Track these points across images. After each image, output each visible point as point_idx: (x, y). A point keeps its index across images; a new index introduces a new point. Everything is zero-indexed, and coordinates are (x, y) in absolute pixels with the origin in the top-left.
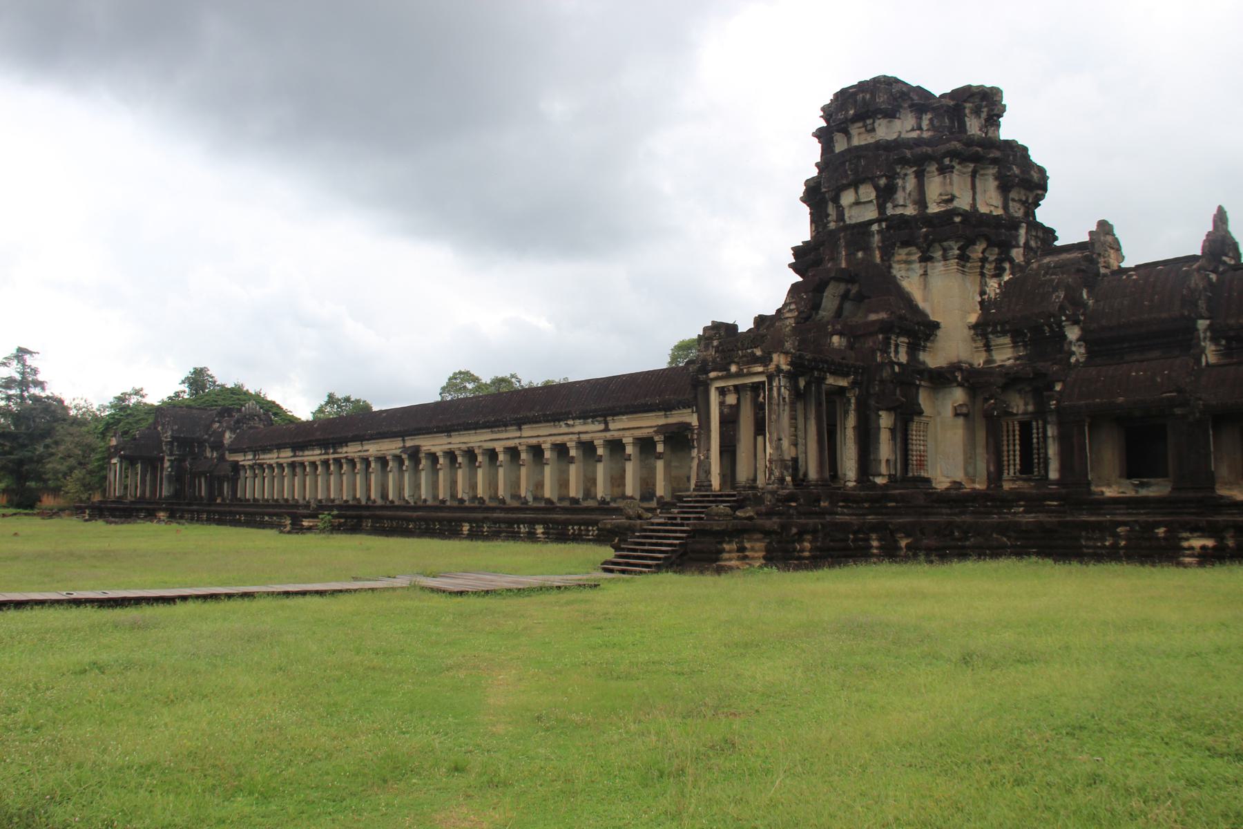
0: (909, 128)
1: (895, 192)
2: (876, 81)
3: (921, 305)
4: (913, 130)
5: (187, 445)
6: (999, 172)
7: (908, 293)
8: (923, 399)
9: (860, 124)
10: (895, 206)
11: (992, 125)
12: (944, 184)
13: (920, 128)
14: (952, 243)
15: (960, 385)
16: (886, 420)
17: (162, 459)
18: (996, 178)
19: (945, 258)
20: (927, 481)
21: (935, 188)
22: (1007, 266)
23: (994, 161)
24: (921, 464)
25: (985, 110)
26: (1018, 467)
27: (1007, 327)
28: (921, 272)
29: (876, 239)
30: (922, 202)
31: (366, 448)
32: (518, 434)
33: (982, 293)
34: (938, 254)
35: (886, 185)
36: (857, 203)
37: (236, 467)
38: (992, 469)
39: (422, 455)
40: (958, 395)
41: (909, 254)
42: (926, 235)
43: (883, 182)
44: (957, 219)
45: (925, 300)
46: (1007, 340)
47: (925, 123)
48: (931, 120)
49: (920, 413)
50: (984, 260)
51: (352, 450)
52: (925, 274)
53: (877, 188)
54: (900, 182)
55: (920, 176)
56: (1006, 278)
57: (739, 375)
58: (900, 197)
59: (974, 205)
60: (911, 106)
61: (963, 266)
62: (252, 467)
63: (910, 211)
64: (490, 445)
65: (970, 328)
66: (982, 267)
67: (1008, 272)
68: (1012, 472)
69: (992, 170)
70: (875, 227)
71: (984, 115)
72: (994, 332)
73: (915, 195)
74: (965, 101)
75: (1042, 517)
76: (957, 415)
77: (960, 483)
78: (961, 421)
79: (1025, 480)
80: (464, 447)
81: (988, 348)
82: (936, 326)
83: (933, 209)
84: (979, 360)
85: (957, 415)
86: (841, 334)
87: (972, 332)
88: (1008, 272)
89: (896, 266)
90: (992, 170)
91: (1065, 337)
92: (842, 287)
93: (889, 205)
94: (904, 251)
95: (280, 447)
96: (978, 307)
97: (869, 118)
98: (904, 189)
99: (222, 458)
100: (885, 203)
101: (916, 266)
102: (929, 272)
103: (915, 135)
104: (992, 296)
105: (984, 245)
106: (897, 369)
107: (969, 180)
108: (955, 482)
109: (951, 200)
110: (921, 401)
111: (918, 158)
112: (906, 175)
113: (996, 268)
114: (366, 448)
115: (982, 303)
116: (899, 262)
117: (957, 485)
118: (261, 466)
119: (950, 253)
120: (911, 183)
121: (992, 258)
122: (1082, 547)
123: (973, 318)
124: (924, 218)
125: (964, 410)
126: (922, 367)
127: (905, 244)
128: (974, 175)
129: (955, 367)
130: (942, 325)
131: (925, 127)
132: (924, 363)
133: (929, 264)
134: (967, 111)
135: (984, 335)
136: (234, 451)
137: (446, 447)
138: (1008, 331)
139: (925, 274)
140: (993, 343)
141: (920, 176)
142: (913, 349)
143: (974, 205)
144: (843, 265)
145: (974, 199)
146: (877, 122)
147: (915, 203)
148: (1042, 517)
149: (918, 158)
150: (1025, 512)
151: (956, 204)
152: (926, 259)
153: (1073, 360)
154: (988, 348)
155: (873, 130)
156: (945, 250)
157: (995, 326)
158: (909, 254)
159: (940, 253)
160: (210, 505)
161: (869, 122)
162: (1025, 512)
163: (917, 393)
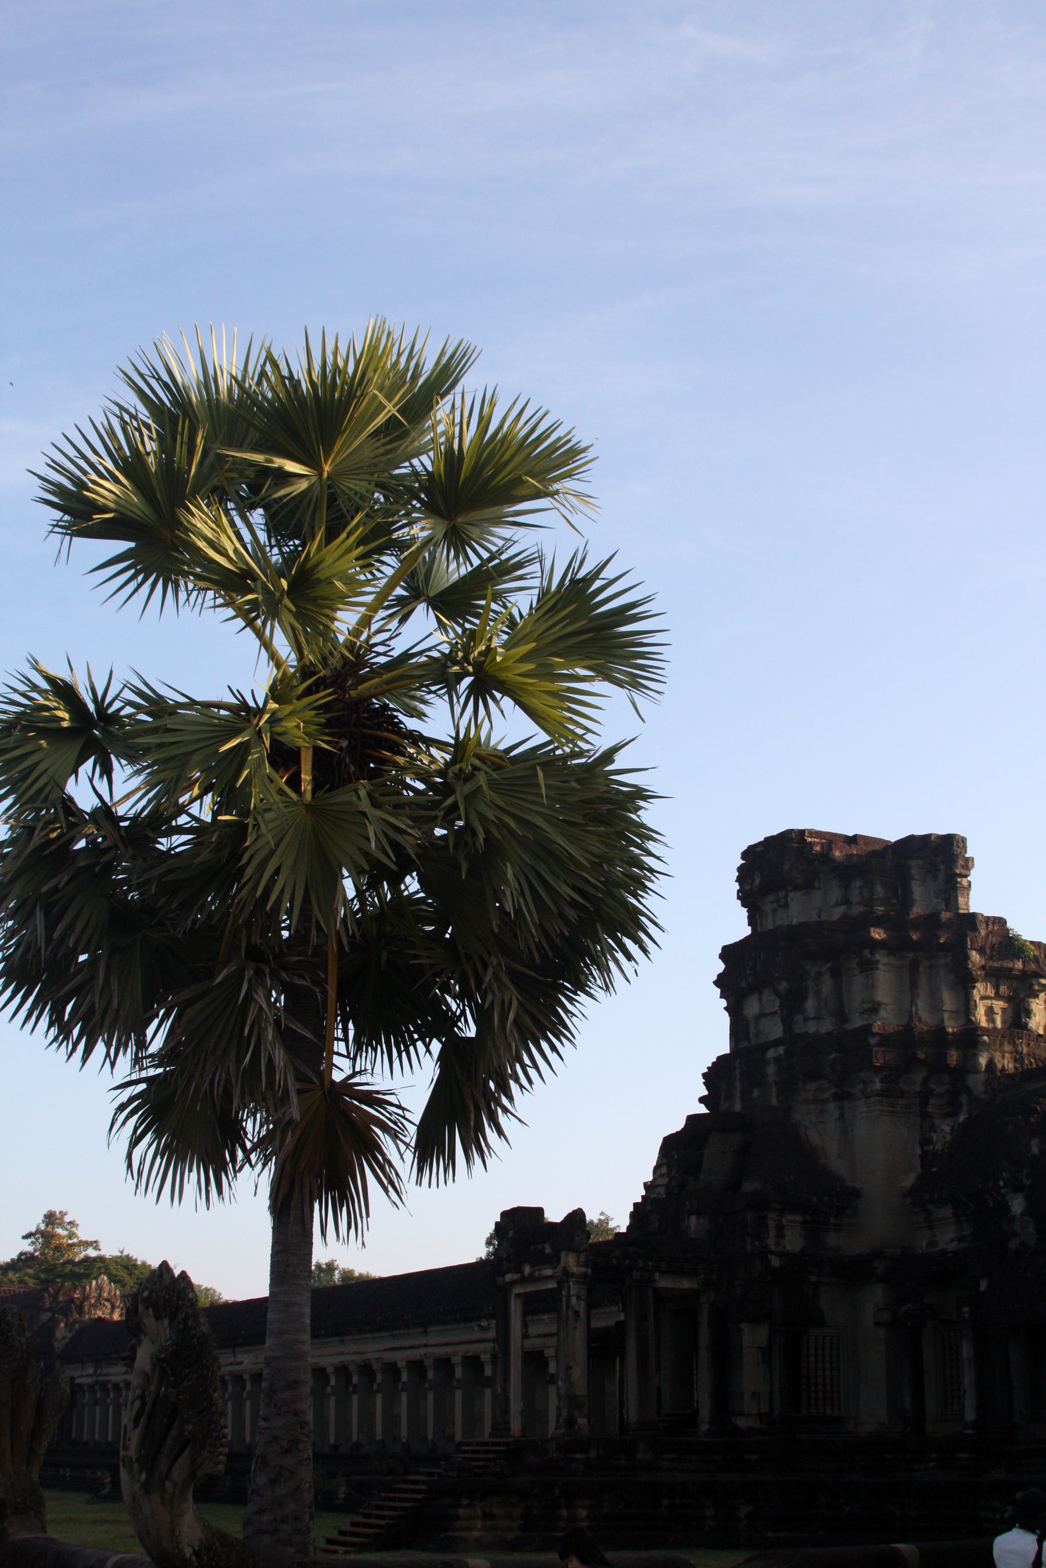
9: (772, 898)
22: (964, 1099)
28: (836, 1115)
29: (771, 1070)
31: (239, 1358)
32: (422, 1341)
33: (925, 1142)
36: (763, 1015)
43: (783, 986)
46: (947, 1212)
52: (841, 1117)
53: (778, 994)
55: (836, 974)
56: (962, 1118)
57: (532, 1279)
58: (810, 1005)
62: (91, 1387)
64: (389, 1356)
67: (965, 1108)
70: (771, 1054)
71: (941, 875)
76: (877, 1324)
80: (358, 1358)
85: (877, 1324)
86: (699, 1213)
88: (965, 1108)
91: (1007, 1208)
94: (812, 1086)
96: (918, 1164)
98: (818, 994)
101: (832, 1106)
104: (939, 1147)
105: (923, 1073)
114: (239, 1358)
115: (923, 1156)
118: (103, 1385)
120: (827, 985)
123: (909, 1181)
128: (914, 967)
134: (915, 872)
137: (337, 1359)
144: (738, 1108)
146: (791, 895)
152: (842, 1097)
153: (1013, 1244)
155: (786, 906)
161: (782, 894)
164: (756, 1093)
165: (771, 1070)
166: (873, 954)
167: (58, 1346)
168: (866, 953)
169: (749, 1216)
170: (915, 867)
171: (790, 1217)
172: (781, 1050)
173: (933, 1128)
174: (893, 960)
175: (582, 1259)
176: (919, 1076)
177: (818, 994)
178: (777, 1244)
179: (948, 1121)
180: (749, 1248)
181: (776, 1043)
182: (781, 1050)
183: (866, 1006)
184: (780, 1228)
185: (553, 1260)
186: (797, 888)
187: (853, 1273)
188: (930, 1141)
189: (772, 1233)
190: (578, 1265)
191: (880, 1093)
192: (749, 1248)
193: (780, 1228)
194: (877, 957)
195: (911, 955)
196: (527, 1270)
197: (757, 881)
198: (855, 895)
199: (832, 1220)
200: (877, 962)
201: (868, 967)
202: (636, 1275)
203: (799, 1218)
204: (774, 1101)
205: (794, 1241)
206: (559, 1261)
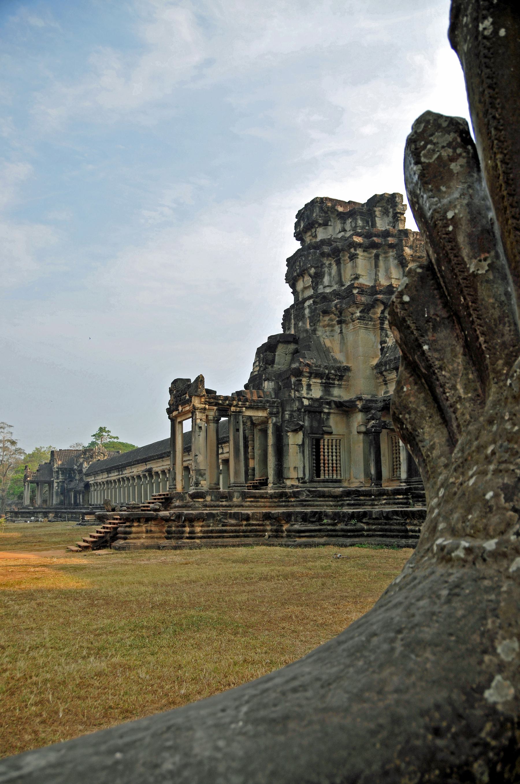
2: (313, 202)
4: (340, 232)
5: (68, 472)
8: (335, 423)
9: (309, 234)
10: (324, 287)
13: (344, 230)
15: (361, 411)
16: (294, 440)
17: (53, 481)
18: (395, 258)
24: (335, 470)
25: (391, 210)
27: (392, 366)
28: (339, 331)
29: (307, 311)
33: (383, 342)
35: (316, 273)
37: (87, 486)
39: (153, 473)
44: (355, 291)
47: (348, 227)
50: (382, 320)
51: (127, 473)
52: (341, 332)
53: (310, 275)
54: (326, 269)
55: (338, 263)
58: (326, 280)
61: (367, 324)
66: (382, 323)
69: (392, 253)
71: (391, 214)
72: (386, 370)
73: (337, 279)
82: (348, 369)
87: (375, 371)
89: (320, 329)
90: (392, 253)
92: (292, 347)
93: (321, 287)
94: (327, 318)
95: (102, 471)
97: (312, 228)
98: (330, 274)
99: (81, 480)
100: (317, 284)
102: (344, 331)
105: (382, 308)
106: (306, 402)
109: (357, 278)
111: (339, 251)
115: (382, 349)
116: (324, 326)
122: (407, 531)
123: (375, 362)
125: (363, 429)
127: (326, 312)
128: (377, 257)
131: (348, 230)
133: (344, 326)
134: (377, 213)
135: (381, 373)
136: (88, 475)
137: (161, 468)
139: (341, 332)
142: (327, 387)
144: (293, 332)
145: (376, 275)
146: (318, 230)
149: (339, 251)
151: (361, 281)
155: (316, 236)
160: (74, 509)
161: (313, 230)
163: (328, 419)
164: (300, 324)
165: (307, 311)
166: (355, 250)
167: (84, 470)
168: (352, 250)
169: (293, 380)
170: (378, 211)
171: (314, 380)
172: (311, 301)
173: (387, 336)
174: (365, 254)
175: (203, 400)
176: (379, 309)
177: (330, 274)
178: (308, 394)
180: (293, 396)
181: (309, 298)
182: (311, 301)
183: (353, 277)
184: (309, 386)
185: (189, 401)
186: (320, 225)
187: (346, 409)
188: (385, 342)
189: (305, 388)
190: (201, 403)
191: (360, 318)
192: (293, 396)
193: (309, 386)
194: (358, 252)
195: (375, 251)
196: (180, 408)
197: (302, 226)
198: (348, 227)
199: (336, 382)
201: (353, 257)
202: (233, 409)
203: (319, 381)
204: (308, 327)
205: (317, 393)
206: (191, 402)
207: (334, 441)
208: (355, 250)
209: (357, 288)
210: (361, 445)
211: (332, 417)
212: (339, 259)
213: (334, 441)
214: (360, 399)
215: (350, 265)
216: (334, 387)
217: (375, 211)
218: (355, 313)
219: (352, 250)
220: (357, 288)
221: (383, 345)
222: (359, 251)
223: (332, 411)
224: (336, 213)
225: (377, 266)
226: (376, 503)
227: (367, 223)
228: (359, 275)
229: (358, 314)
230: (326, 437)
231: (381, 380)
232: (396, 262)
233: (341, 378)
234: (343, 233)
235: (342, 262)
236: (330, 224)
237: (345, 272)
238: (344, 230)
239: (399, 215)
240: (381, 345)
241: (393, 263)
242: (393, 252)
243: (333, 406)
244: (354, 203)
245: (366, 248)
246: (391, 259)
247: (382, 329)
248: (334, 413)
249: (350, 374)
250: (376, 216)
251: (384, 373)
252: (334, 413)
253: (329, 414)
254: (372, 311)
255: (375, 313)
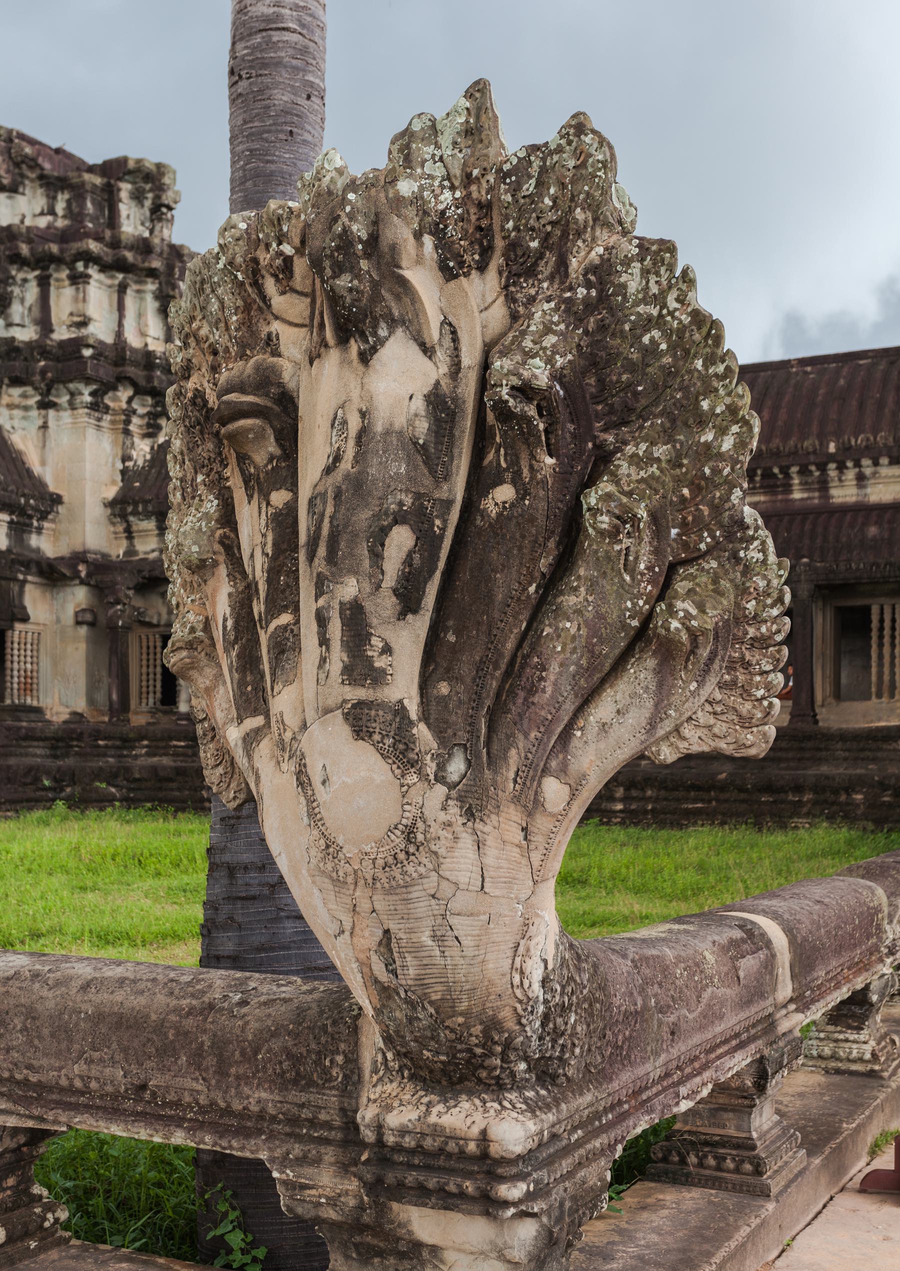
0: (38, 211)
1: (9, 304)
3: (37, 469)
4: (42, 214)
6: (160, 289)
7: (19, 453)
11: (160, 220)
12: (76, 300)
14: (81, 386)
15: (82, 582)
19: (72, 406)
20: (38, 711)
21: (63, 302)
23: (152, 273)
25: (150, 195)
26: (159, 695)
28: (40, 422)
30: (45, 323)
33: (125, 458)
34: (64, 399)
38: (115, 697)
40: (78, 596)
41: (24, 396)
42: (43, 372)
44: (87, 353)
45: (43, 463)
47: (60, 207)
48: (69, 202)
49: (25, 619)
54: (16, 291)
55: (44, 283)
59: (119, 333)
60: (41, 177)
63: (26, 334)
65: (105, 505)
66: (128, 422)
68: (151, 701)
69: (151, 286)
71: (148, 203)
72: (135, 513)
73: (36, 312)
74: (120, 179)
75: (166, 761)
77: (81, 715)
78: (83, 630)
79: (165, 713)
81: (129, 534)
82: (57, 500)
83: (62, 334)
84: (118, 550)
85: (78, 623)
94: (16, 392)
98: (22, 301)
101: (34, 413)
102: (51, 423)
103: (43, 222)
104: (140, 463)
105: (130, 392)
107: (115, 296)
108: (74, 714)
109: (84, 323)
110: (28, 602)
112: (25, 280)
113: (149, 425)
115: (124, 472)
117: (77, 716)
119: (78, 399)
120: (32, 293)
121: (141, 411)
123: (111, 493)
124: (39, 348)
126: (33, 556)
127: (16, 382)
128: (122, 289)
129: (79, 557)
130: (65, 499)
132: (38, 550)
133: (51, 413)
135: (124, 516)
138: (153, 513)
139: (45, 427)
140: (134, 528)
141: (44, 283)
143: (119, 333)
145: (120, 324)
147: (36, 322)
148: (166, 761)
150: (148, 754)
152: (45, 405)
154: (129, 534)
156: (72, 394)
157: (136, 504)
158: (24, 396)
159: (67, 397)
162: (148, 754)
163: (21, 593)
166: (86, 267)
174: (101, 277)
176: (124, 393)
179: (148, 441)
187: (54, 574)
188: (130, 458)
194: (90, 271)
195: (120, 276)
200: (89, 276)
201: (78, 279)
207: (30, 634)
208: (86, 267)
209: (93, 347)
210: (83, 646)
211: (28, 588)
212: (49, 276)
213: (30, 634)
214: (85, 561)
215: (68, 292)
216: (30, 532)
217: (119, 190)
218: (81, 394)
219: (80, 266)
220: (93, 347)
221: (127, 464)
222: (93, 271)
223: (30, 578)
224: (38, 172)
225: (121, 307)
226: (125, 752)
227: (102, 210)
228: (90, 319)
229: (88, 399)
230: (18, 626)
231: (120, 528)
232: (156, 304)
233: (43, 517)
234: (50, 218)
235: (52, 282)
236: (21, 190)
237: (57, 305)
238: (52, 212)
239: (164, 210)
240: (123, 461)
241: (151, 305)
242: (153, 283)
243: (34, 569)
244: (69, 156)
245: (105, 268)
246: (149, 298)
247: (127, 432)
248: (33, 583)
249: (60, 509)
250: (120, 201)
251: (131, 518)
252: (33, 583)
253: (25, 582)
254: (110, 394)
255: (116, 399)
